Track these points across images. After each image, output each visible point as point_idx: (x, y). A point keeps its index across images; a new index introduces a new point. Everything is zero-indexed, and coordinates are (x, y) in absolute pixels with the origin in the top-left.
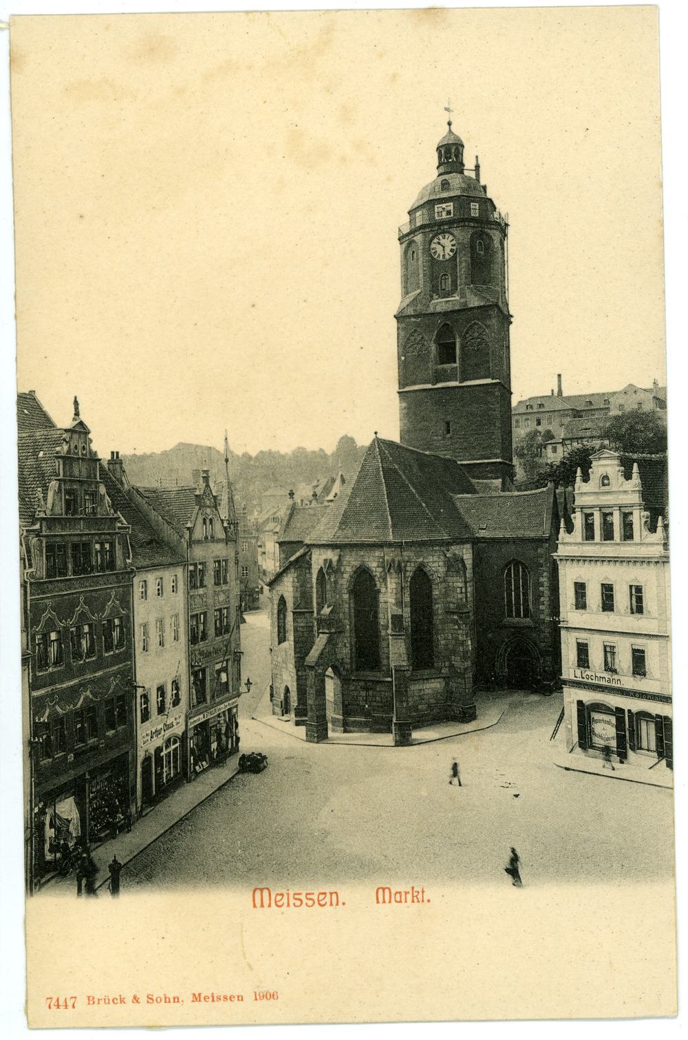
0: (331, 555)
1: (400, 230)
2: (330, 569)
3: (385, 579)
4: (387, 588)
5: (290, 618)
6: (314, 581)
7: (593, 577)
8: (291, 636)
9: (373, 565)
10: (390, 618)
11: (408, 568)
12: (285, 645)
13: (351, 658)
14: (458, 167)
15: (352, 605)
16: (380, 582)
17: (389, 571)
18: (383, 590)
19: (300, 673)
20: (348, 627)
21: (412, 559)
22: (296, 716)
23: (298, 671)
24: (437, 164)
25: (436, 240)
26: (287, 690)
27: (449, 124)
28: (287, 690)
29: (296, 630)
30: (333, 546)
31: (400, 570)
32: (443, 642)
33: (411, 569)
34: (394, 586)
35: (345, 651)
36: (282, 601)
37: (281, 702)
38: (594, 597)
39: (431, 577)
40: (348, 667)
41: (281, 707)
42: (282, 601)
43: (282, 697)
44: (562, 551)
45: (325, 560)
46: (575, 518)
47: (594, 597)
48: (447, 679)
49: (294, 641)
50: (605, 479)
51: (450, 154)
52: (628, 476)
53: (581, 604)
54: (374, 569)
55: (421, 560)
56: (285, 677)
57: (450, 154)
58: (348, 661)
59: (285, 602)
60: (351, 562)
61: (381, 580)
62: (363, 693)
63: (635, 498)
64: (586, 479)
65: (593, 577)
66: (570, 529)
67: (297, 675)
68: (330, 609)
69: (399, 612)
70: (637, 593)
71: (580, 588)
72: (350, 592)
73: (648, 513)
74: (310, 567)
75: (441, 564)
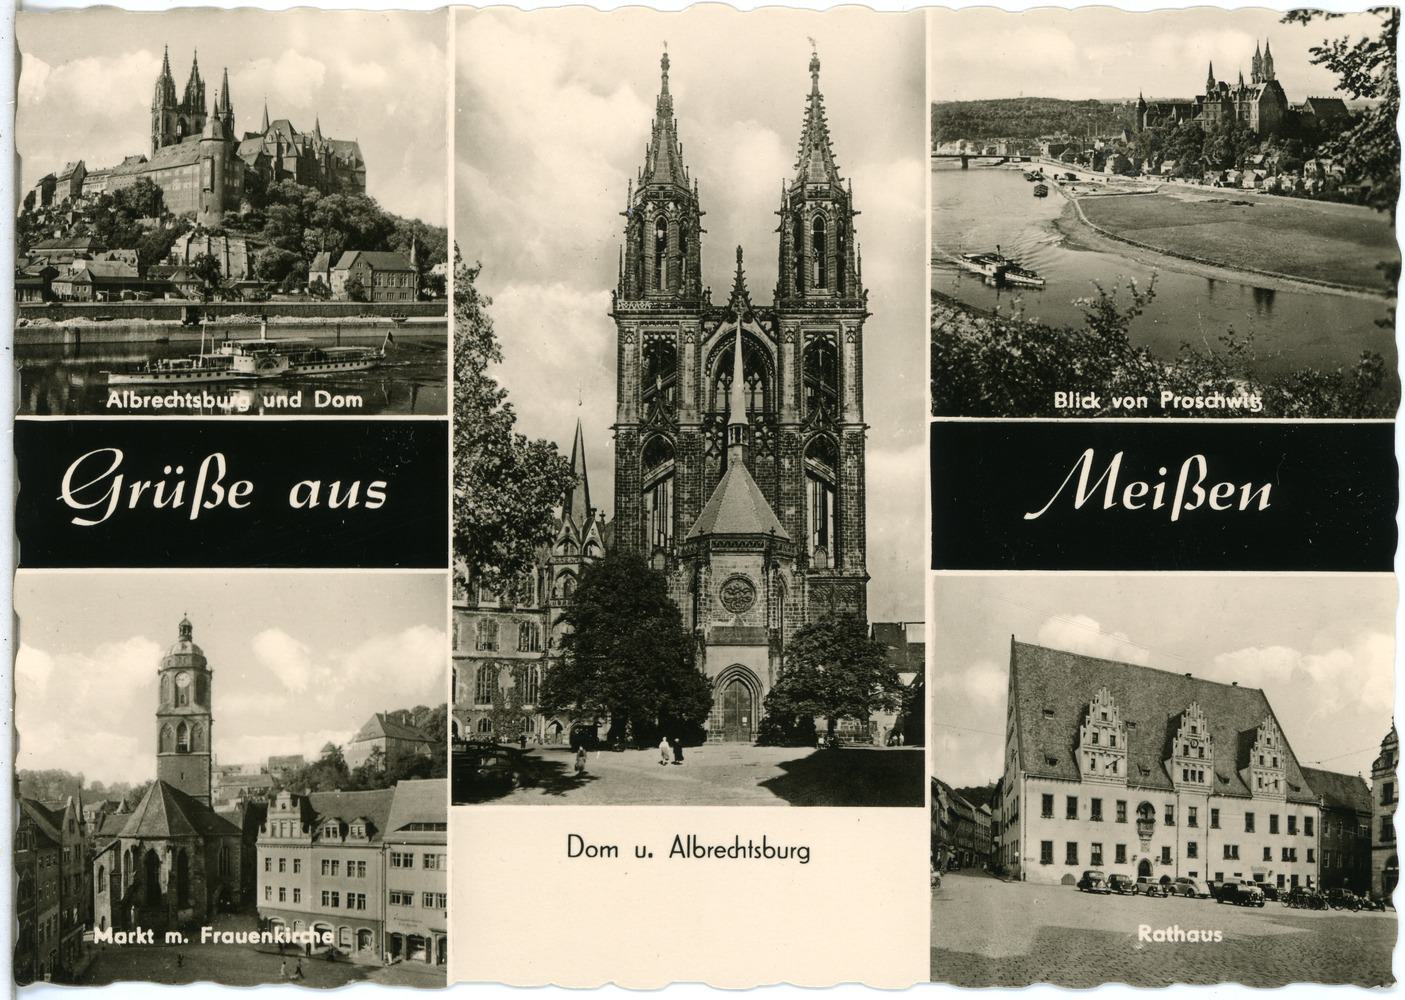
2: (136, 850)
3: (164, 856)
7: (276, 854)
8: (108, 889)
12: (103, 893)
21: (180, 846)
28: (103, 918)
31: (174, 850)
33: (178, 849)
35: (141, 895)
38: (275, 866)
42: (102, 869)
44: (259, 840)
50: (284, 807)
52: (294, 804)
65: (276, 854)
66: (264, 830)
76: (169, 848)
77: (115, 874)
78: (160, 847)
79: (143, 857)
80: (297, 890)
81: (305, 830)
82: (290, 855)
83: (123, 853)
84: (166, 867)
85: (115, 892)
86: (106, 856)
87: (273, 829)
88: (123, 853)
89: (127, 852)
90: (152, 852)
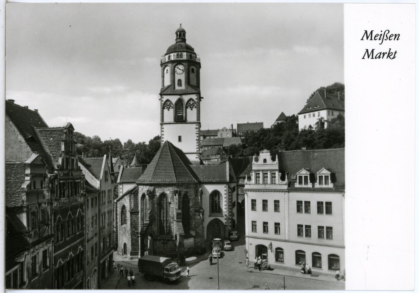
0: (152, 188)
1: (161, 62)
2: (152, 194)
3: (172, 198)
4: (173, 201)
5: (128, 215)
6: (140, 199)
7: (259, 197)
8: (129, 222)
9: (168, 192)
10: (175, 213)
11: (182, 194)
12: (123, 226)
13: (158, 231)
14: (184, 40)
15: (158, 209)
16: (171, 200)
17: (175, 195)
18: (172, 203)
19: (133, 237)
20: (156, 218)
21: (184, 190)
22: (131, 255)
23: (132, 236)
24: (176, 38)
25: (177, 67)
26: (125, 244)
27: (181, 24)
28: (125, 244)
29: (131, 220)
30: (151, 185)
32: (194, 223)
33: (183, 193)
34: (177, 201)
35: (155, 228)
36: (124, 207)
37: (122, 250)
38: (259, 205)
39: (190, 197)
40: (156, 234)
41: (122, 252)
43: (123, 247)
44: (246, 187)
45: (148, 191)
46: (252, 175)
47: (259, 205)
48: (194, 237)
49: (131, 224)
50: (265, 161)
51: (181, 35)
52: (273, 159)
53: (254, 207)
54: (168, 194)
55: (186, 190)
56: (124, 239)
57: (181, 35)
58: (156, 232)
59: (125, 207)
60: (158, 192)
61: (171, 199)
62: (163, 245)
63: (277, 168)
64: (257, 160)
65: (259, 197)
66: (249, 178)
67: (131, 238)
68: (150, 211)
69: (180, 211)
70: (277, 203)
71: (254, 202)
72: (158, 204)
73: (280, 173)
74: (138, 193)
75: (194, 192)
76: (175, 193)
77: (134, 212)
78: (168, 191)
79: (155, 199)
80: (277, 225)
81: (283, 178)
82: (271, 198)
83: (140, 195)
84: (173, 209)
85: (134, 226)
86: (127, 198)
87: (257, 177)
88: (140, 195)
89: (144, 196)
90: (163, 195)
